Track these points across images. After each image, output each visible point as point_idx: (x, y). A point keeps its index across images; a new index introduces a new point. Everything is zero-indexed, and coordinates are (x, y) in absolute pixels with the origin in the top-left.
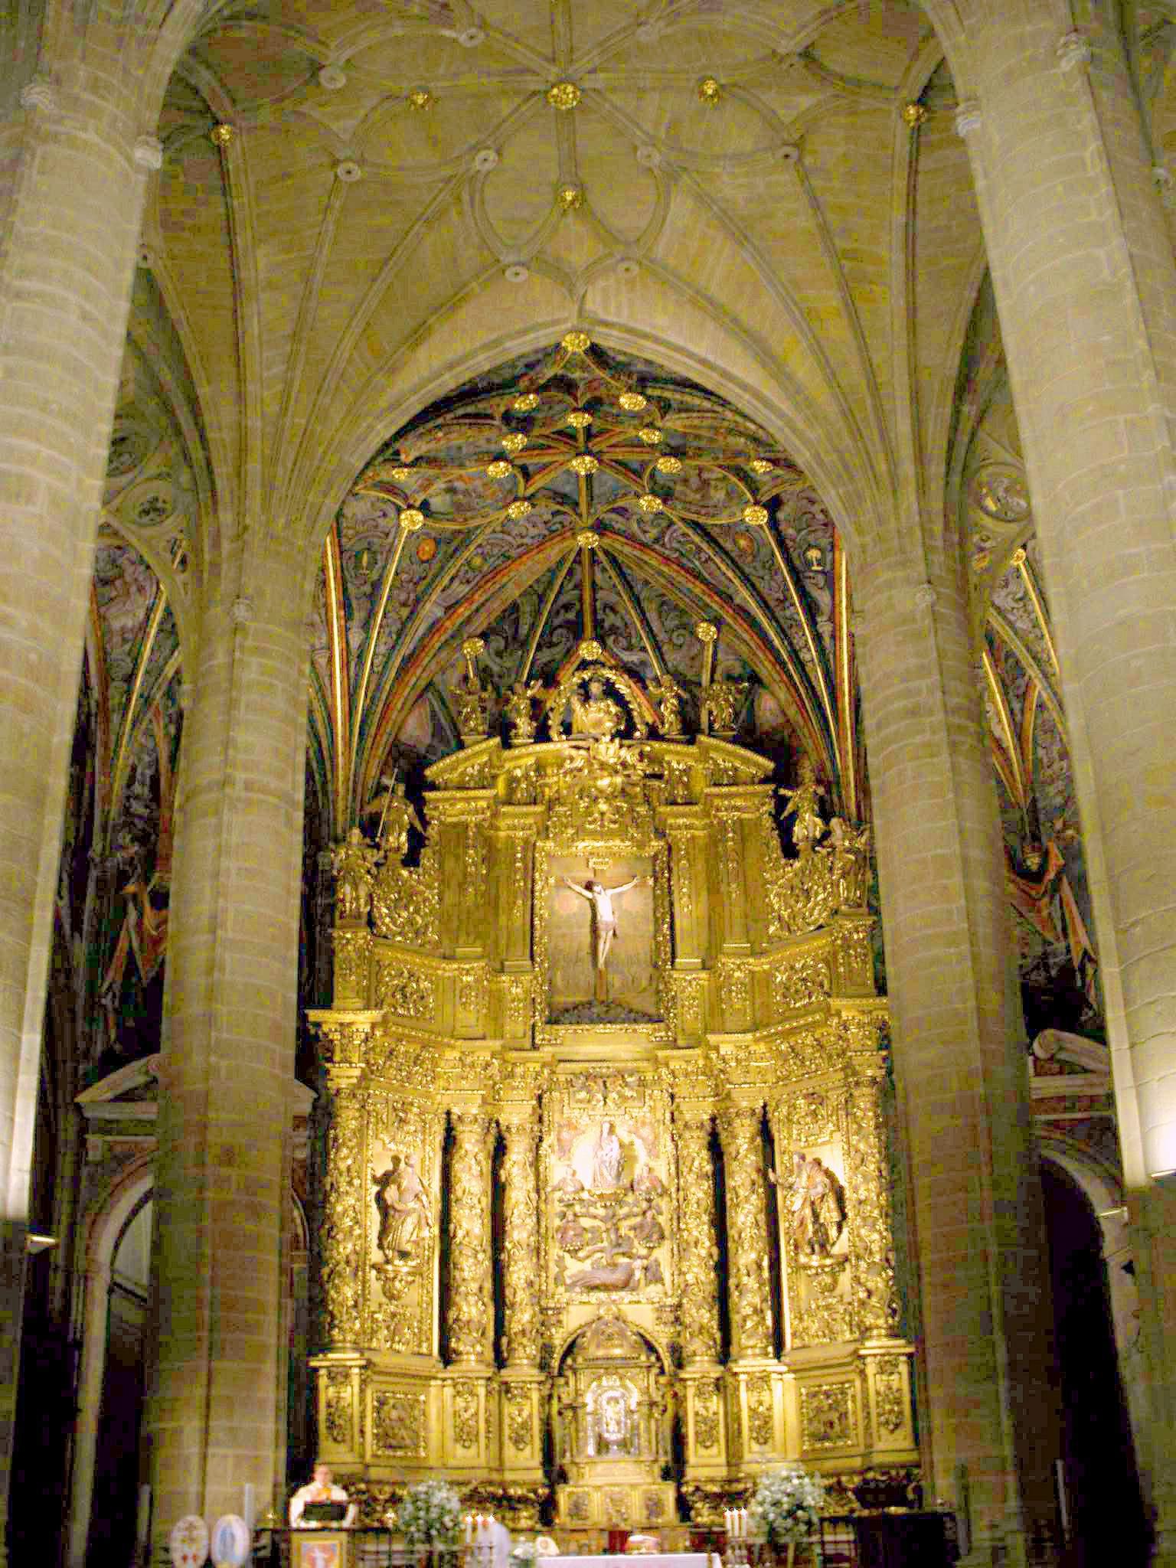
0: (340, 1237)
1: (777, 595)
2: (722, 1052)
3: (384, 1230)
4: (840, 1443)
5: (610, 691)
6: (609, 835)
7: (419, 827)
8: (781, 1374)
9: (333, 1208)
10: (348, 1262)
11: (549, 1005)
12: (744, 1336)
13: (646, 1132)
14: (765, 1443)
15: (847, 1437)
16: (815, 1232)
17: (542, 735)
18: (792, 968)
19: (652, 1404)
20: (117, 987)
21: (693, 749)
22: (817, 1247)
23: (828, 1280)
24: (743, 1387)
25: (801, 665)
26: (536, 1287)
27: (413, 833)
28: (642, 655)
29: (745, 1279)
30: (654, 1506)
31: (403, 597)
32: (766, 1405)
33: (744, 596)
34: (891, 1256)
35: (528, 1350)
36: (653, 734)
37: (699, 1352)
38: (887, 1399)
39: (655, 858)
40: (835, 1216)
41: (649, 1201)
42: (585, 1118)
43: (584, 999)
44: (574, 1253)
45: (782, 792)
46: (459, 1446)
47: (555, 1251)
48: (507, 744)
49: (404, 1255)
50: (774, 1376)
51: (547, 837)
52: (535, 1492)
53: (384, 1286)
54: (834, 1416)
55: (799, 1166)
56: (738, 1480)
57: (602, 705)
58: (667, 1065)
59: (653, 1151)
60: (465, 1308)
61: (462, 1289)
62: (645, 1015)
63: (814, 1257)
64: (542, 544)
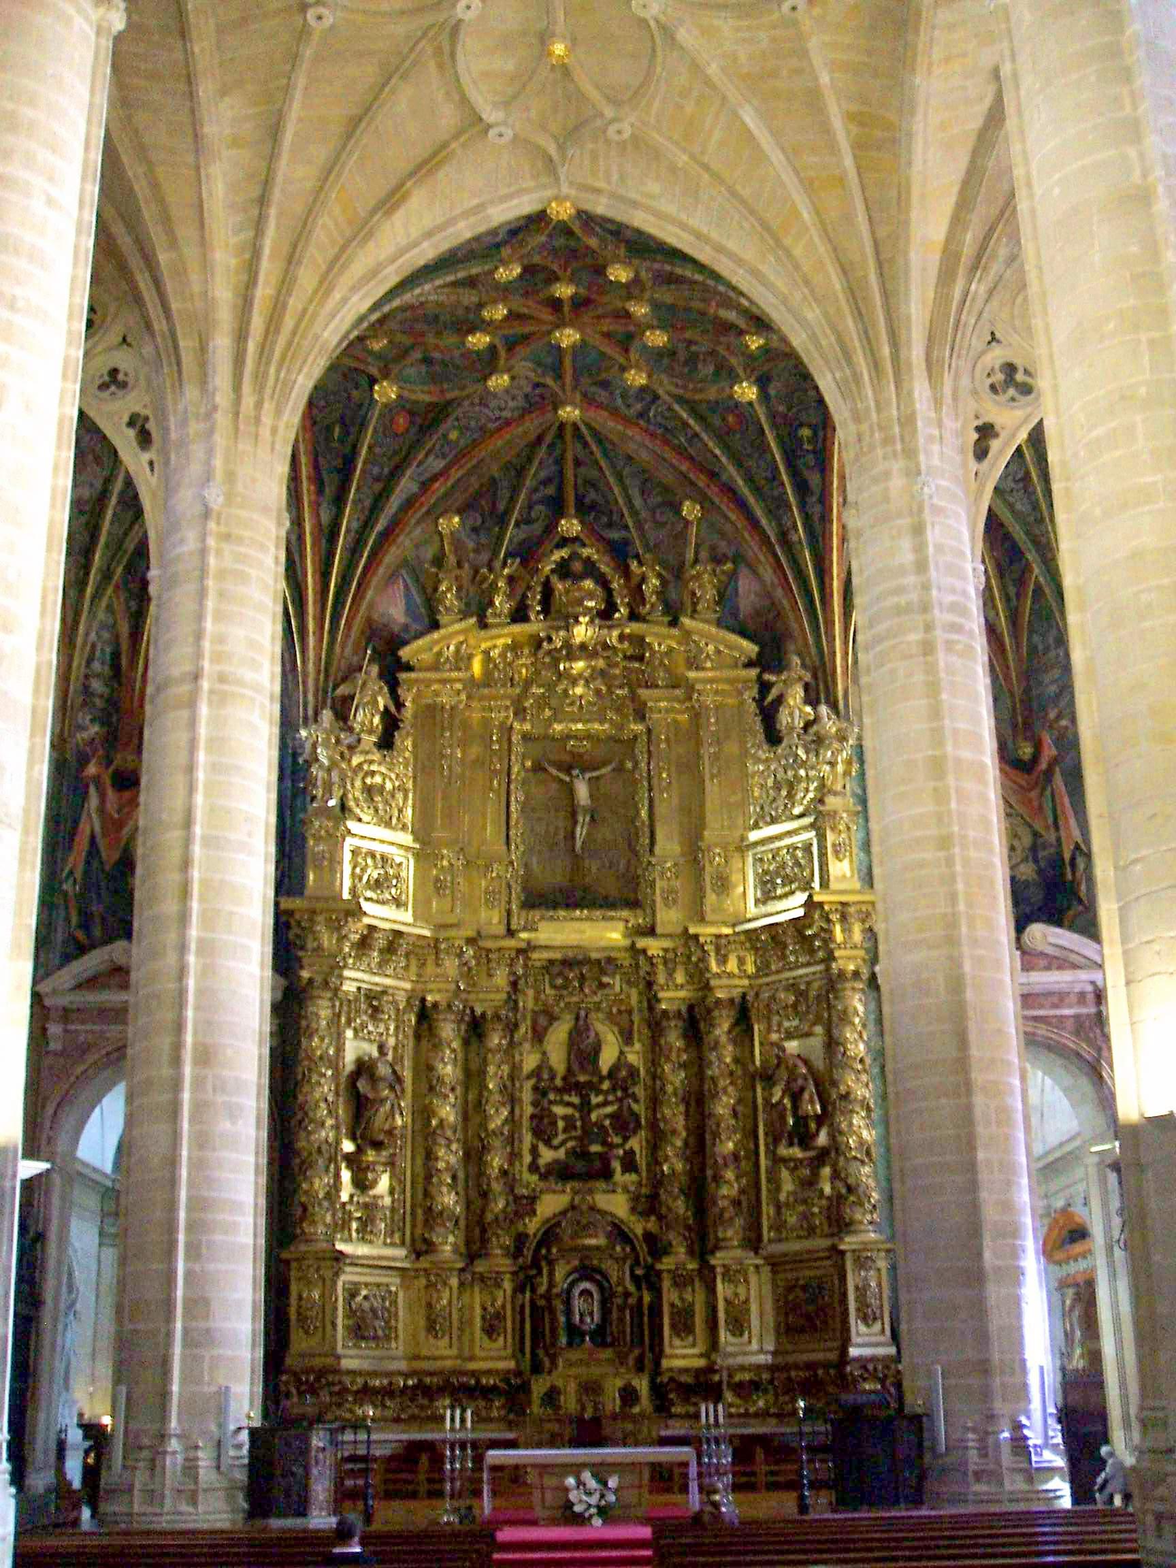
17: (519, 615)
20: (78, 874)
21: (675, 632)
28: (623, 534)
31: (376, 470)
33: (731, 471)
48: (483, 625)
64: (522, 416)
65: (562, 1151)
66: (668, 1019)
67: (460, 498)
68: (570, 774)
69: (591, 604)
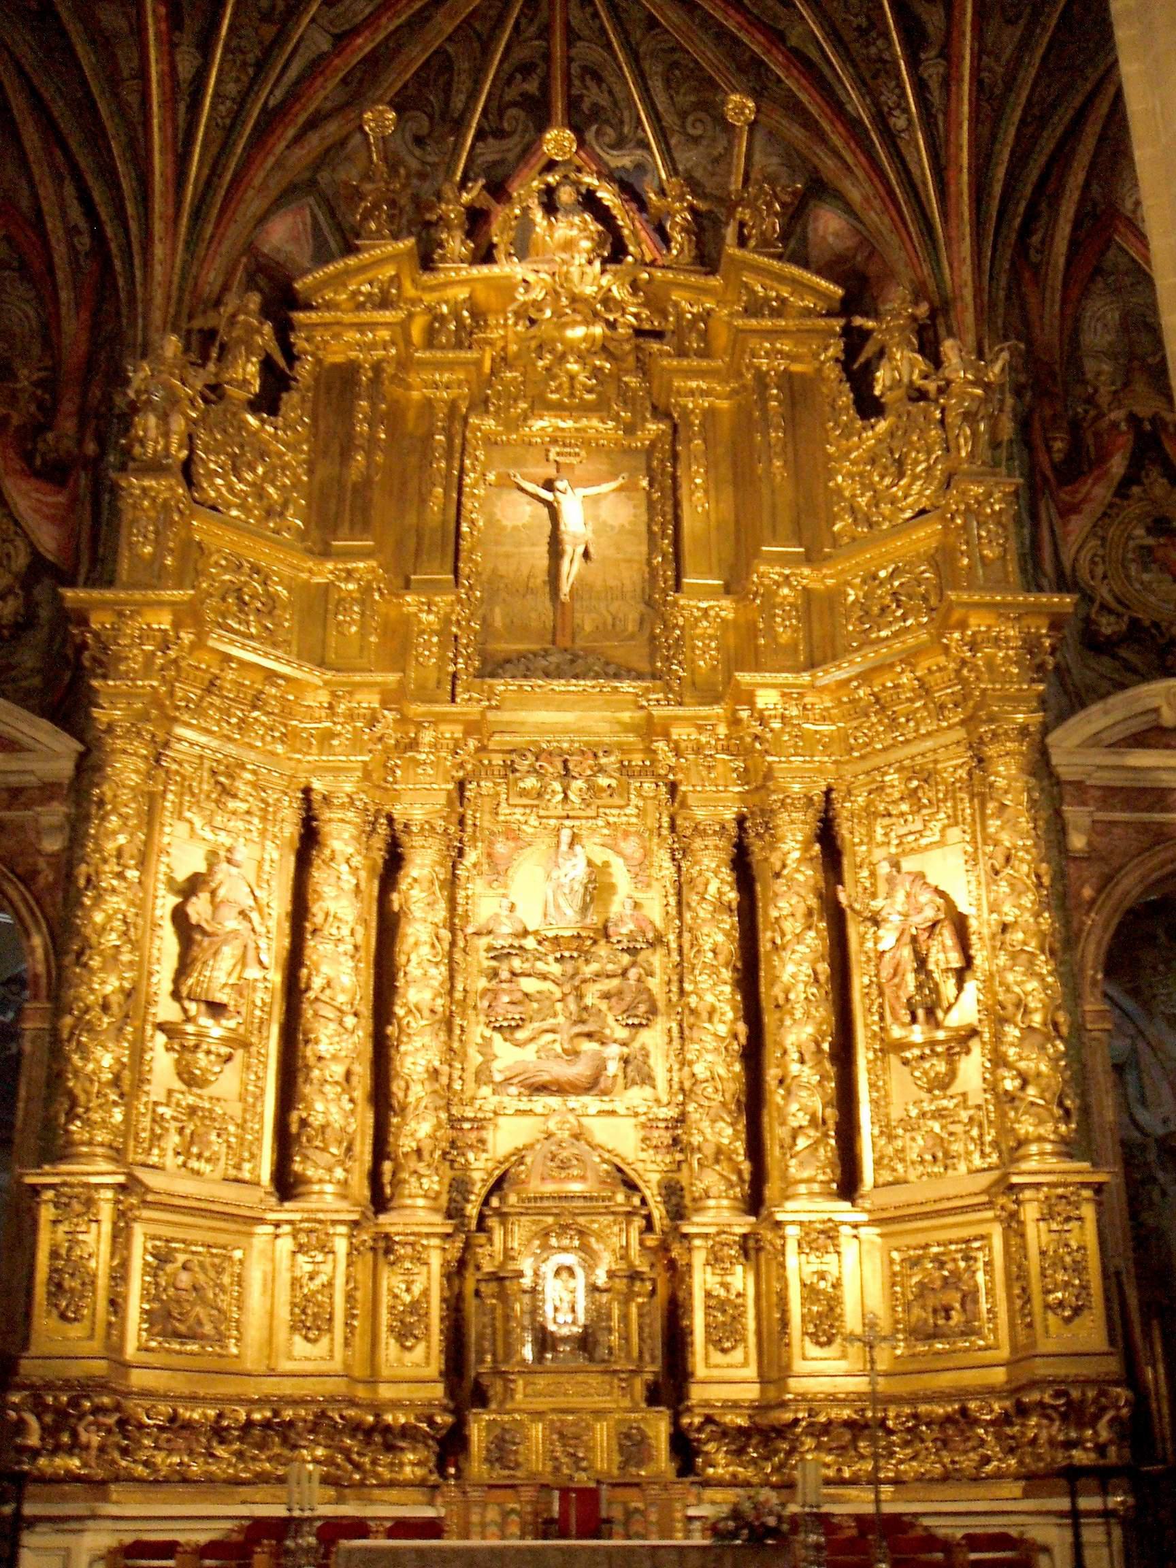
0: (95, 963)
1: (856, 22)
2: (760, 704)
3: (183, 970)
4: (963, 1344)
5: (590, 202)
6: (586, 409)
7: (282, 363)
8: (855, 1226)
10: (105, 1007)
12: (793, 1162)
13: (631, 846)
14: (829, 1342)
15: (977, 1333)
16: (920, 987)
18: (875, 577)
19: (634, 1276)
22: (921, 1013)
23: (942, 1067)
24: (791, 1247)
25: (890, 138)
26: (444, 1080)
27: (267, 365)
28: (639, 153)
29: (794, 1068)
32: (831, 1279)
34: (1061, 1017)
35: (426, 1183)
37: (714, 1192)
38: (1058, 1263)
39: (650, 451)
40: (956, 961)
42: (533, 821)
43: (535, 647)
44: (508, 1030)
45: (858, 321)
46: (298, 1339)
47: (478, 1031)
49: (216, 1009)
51: (487, 411)
52: (431, 1422)
53: (178, 1062)
54: (954, 1298)
55: (890, 880)
56: (783, 1405)
57: (577, 220)
58: (667, 736)
59: (641, 871)
60: (319, 1106)
61: (316, 1073)
62: (629, 671)
63: (917, 1028)
66: (703, 834)
67: (396, 79)
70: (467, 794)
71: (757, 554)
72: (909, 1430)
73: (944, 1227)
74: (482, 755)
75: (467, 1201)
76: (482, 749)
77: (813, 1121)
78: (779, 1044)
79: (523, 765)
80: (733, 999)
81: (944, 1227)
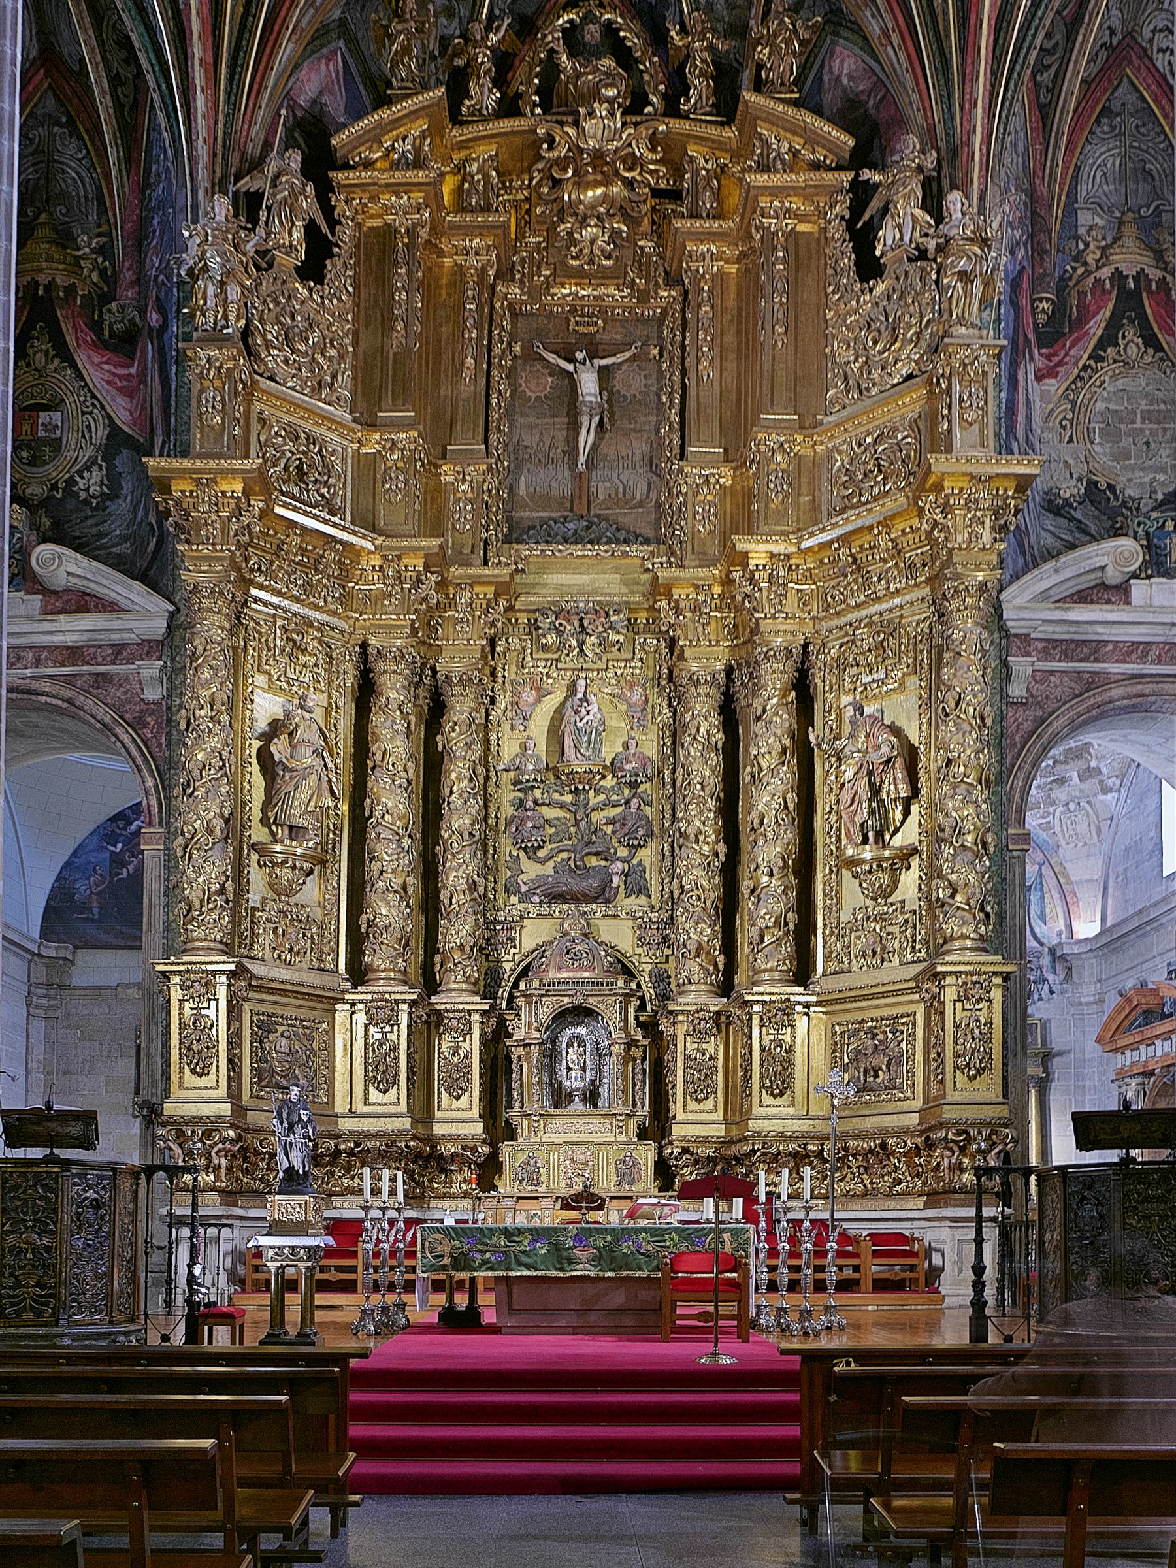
6: (604, 276)
9: (191, 751)
11: (508, 520)
24: (756, 1021)
30: (627, 1171)
36: (672, 110)
41: (633, 785)
47: (506, 849)
50: (799, 1008)
65: (549, 869)
68: (571, 360)
69: (611, 92)
70: (498, 649)
71: (756, 421)
72: (838, 1159)
73: (878, 1007)
74: (510, 615)
75: (500, 986)
76: (510, 608)
77: (777, 923)
78: (750, 860)
79: (545, 623)
80: (716, 823)
81: (878, 1007)
